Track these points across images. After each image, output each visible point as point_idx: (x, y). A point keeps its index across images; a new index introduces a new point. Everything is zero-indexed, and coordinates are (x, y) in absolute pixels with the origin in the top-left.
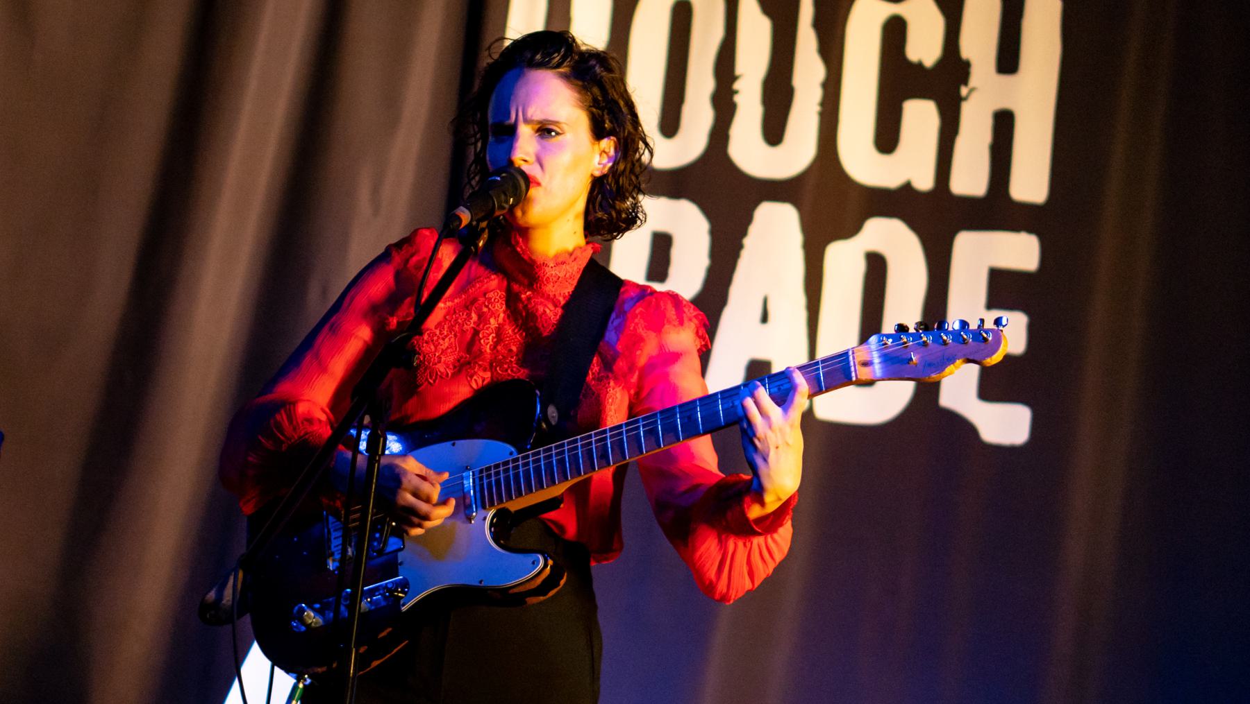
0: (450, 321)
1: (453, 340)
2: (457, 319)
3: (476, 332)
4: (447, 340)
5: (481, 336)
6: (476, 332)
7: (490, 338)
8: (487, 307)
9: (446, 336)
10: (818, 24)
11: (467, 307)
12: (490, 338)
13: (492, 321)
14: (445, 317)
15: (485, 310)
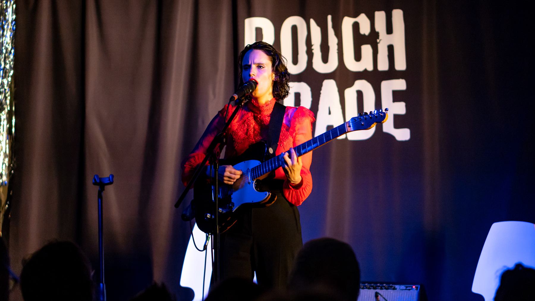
0: (240, 128)
1: (241, 133)
2: (241, 127)
3: (248, 130)
4: (240, 133)
5: (249, 130)
6: (248, 130)
7: (252, 130)
8: (249, 122)
9: (239, 132)
10: (334, 27)
11: (244, 123)
12: (252, 130)
13: (251, 125)
14: (238, 127)
15: (249, 123)
